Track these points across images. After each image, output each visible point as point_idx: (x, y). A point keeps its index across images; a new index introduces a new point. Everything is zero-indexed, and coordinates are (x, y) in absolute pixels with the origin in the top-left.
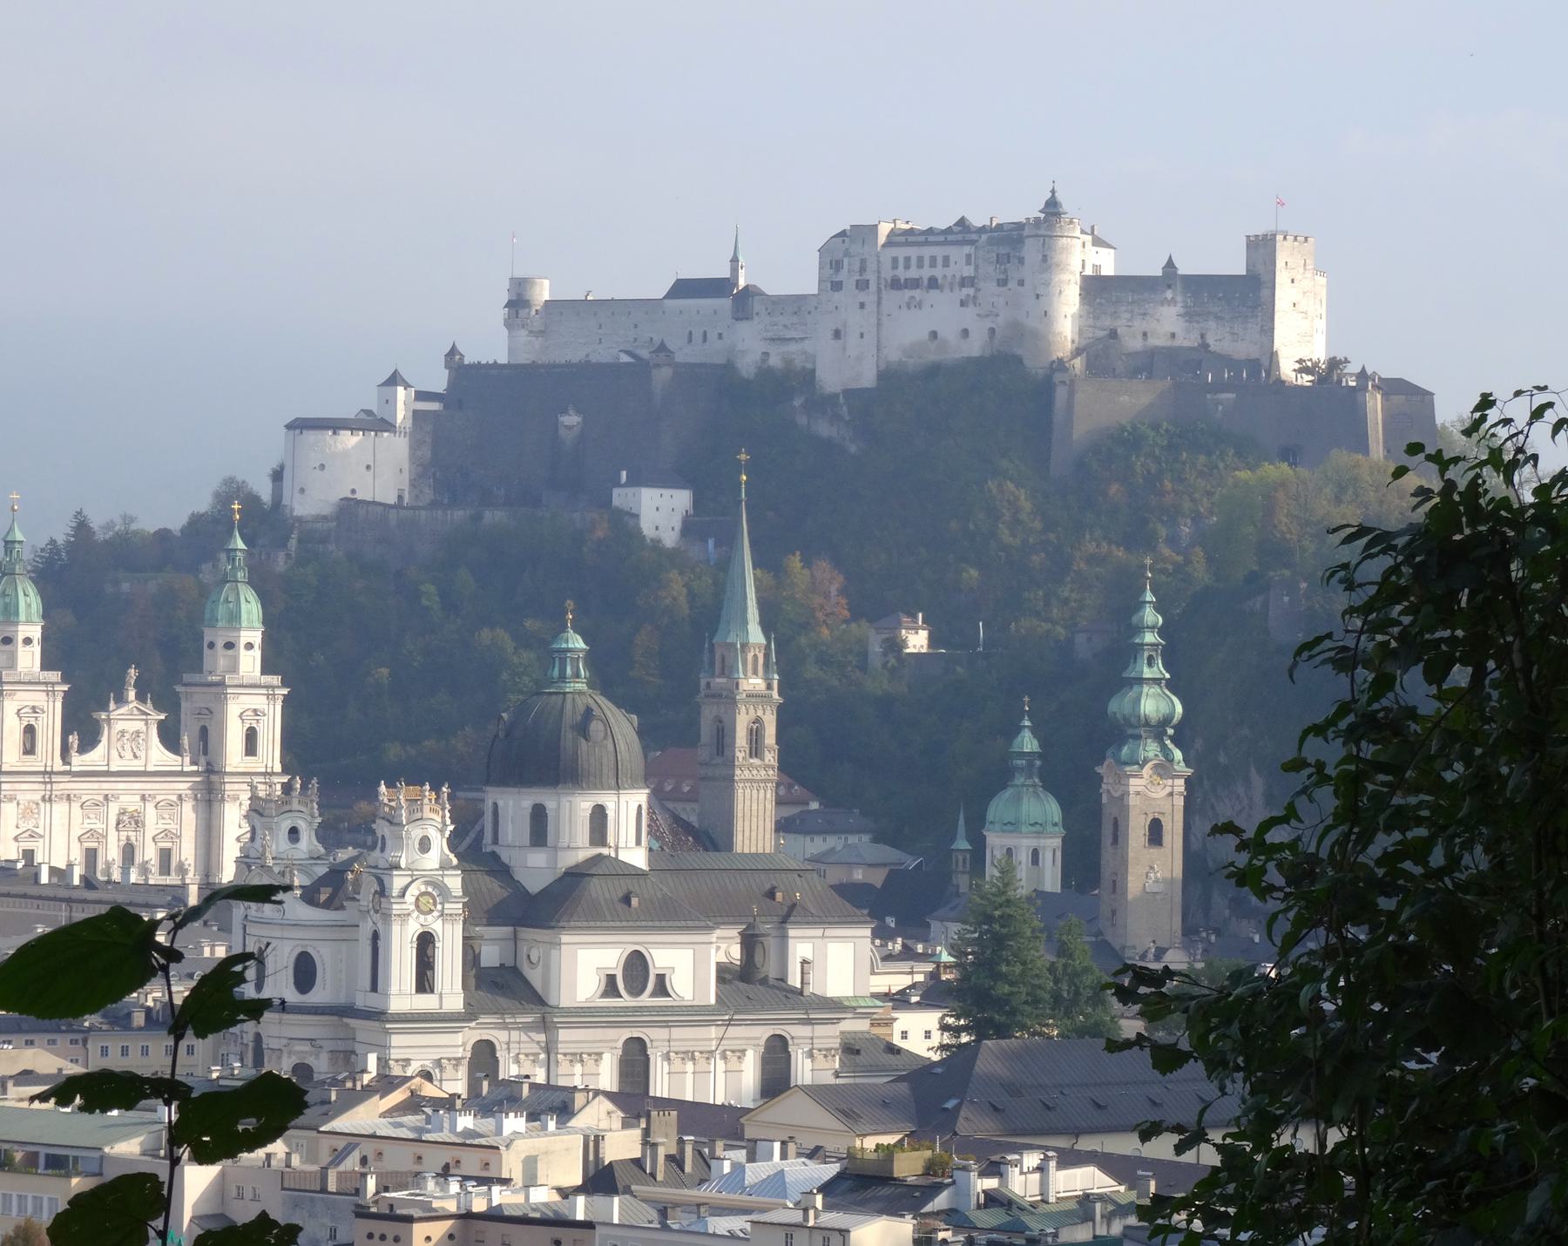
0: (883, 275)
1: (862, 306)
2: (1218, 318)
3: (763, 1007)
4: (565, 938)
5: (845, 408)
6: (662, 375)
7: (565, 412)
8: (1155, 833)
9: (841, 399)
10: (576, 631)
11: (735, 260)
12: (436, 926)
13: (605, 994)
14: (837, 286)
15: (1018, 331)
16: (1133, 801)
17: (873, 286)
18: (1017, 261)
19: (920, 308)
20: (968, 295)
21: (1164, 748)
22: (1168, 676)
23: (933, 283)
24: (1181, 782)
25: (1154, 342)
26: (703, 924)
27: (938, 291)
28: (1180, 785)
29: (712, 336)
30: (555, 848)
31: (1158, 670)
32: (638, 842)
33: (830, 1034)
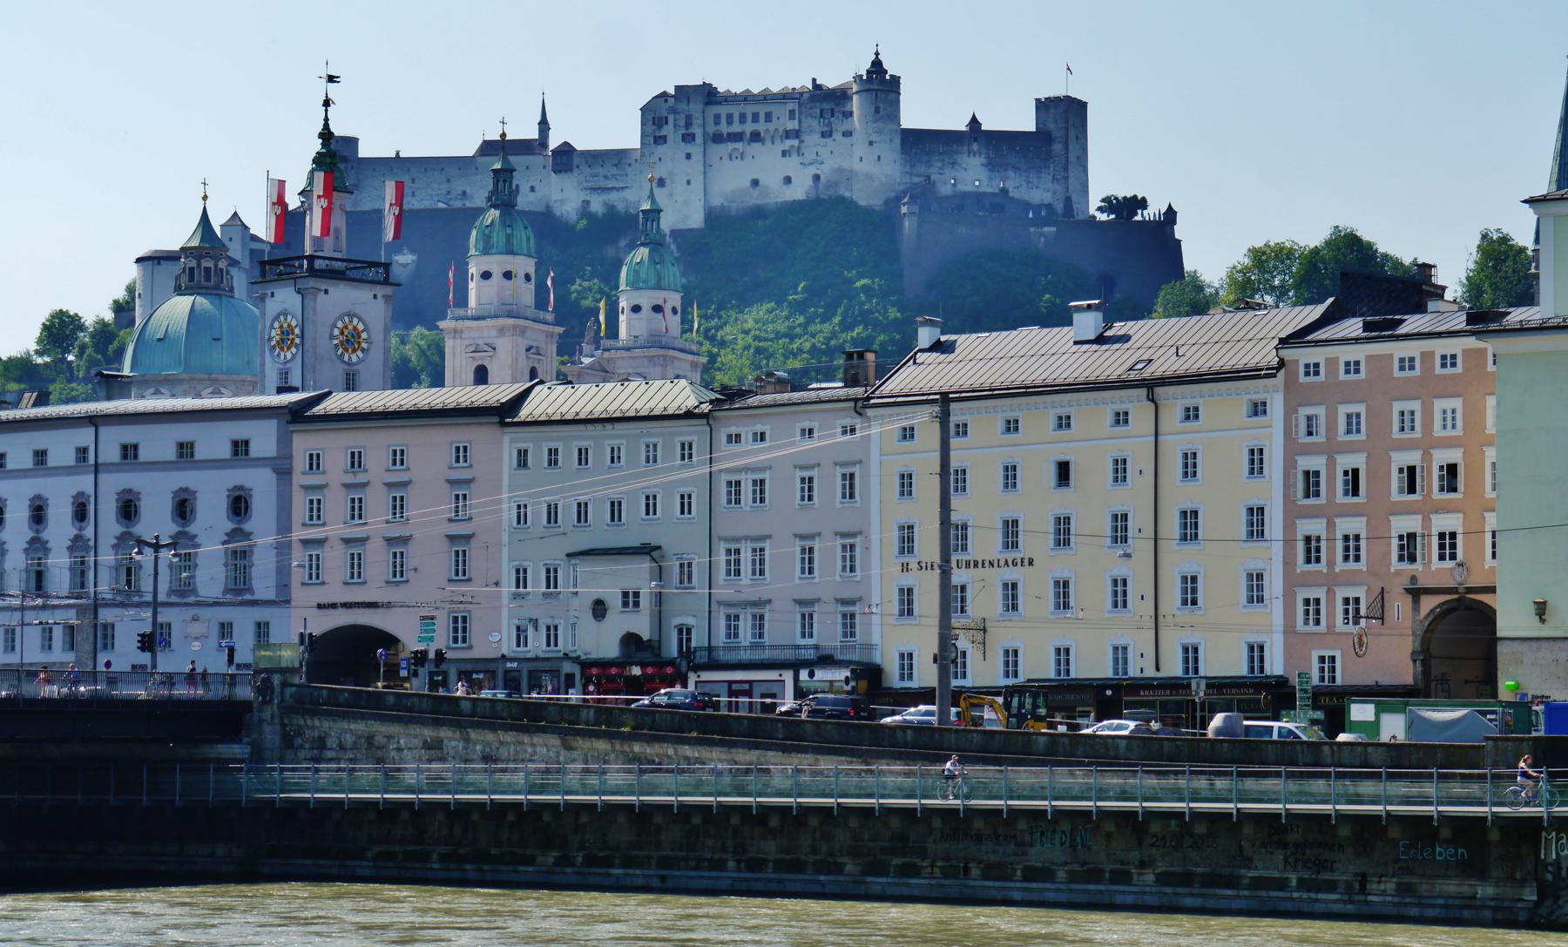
0: (707, 130)
1: (688, 156)
2: (1016, 169)
5: (673, 247)
7: (399, 251)
9: (668, 237)
11: (544, 125)
14: (660, 140)
15: (848, 176)
17: (699, 139)
18: (841, 115)
19: (742, 159)
20: (793, 146)
23: (756, 137)
25: (962, 188)
27: (759, 144)
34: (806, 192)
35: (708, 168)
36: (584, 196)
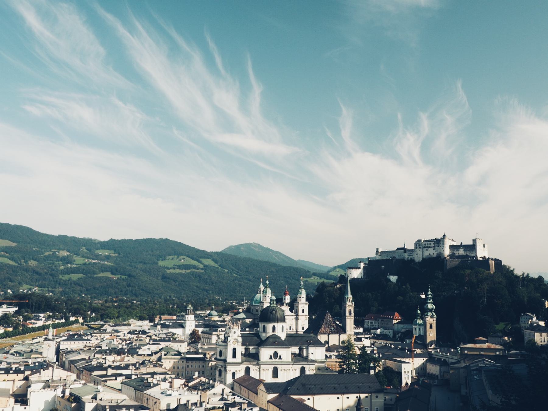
1: (420, 250)
2: (469, 251)
3: (300, 361)
4: (262, 349)
6: (394, 261)
7: (382, 266)
8: (431, 327)
10: (274, 296)
11: (405, 245)
12: (235, 346)
13: (270, 359)
14: (417, 248)
16: (427, 321)
17: (421, 248)
21: (432, 314)
22: (432, 302)
23: (429, 247)
24: (435, 319)
25: (459, 254)
26: (288, 347)
28: (435, 319)
29: (402, 255)
30: (266, 333)
31: (431, 301)
32: (283, 331)
33: (313, 367)
34: (436, 256)
35: (423, 252)
36: (407, 257)
